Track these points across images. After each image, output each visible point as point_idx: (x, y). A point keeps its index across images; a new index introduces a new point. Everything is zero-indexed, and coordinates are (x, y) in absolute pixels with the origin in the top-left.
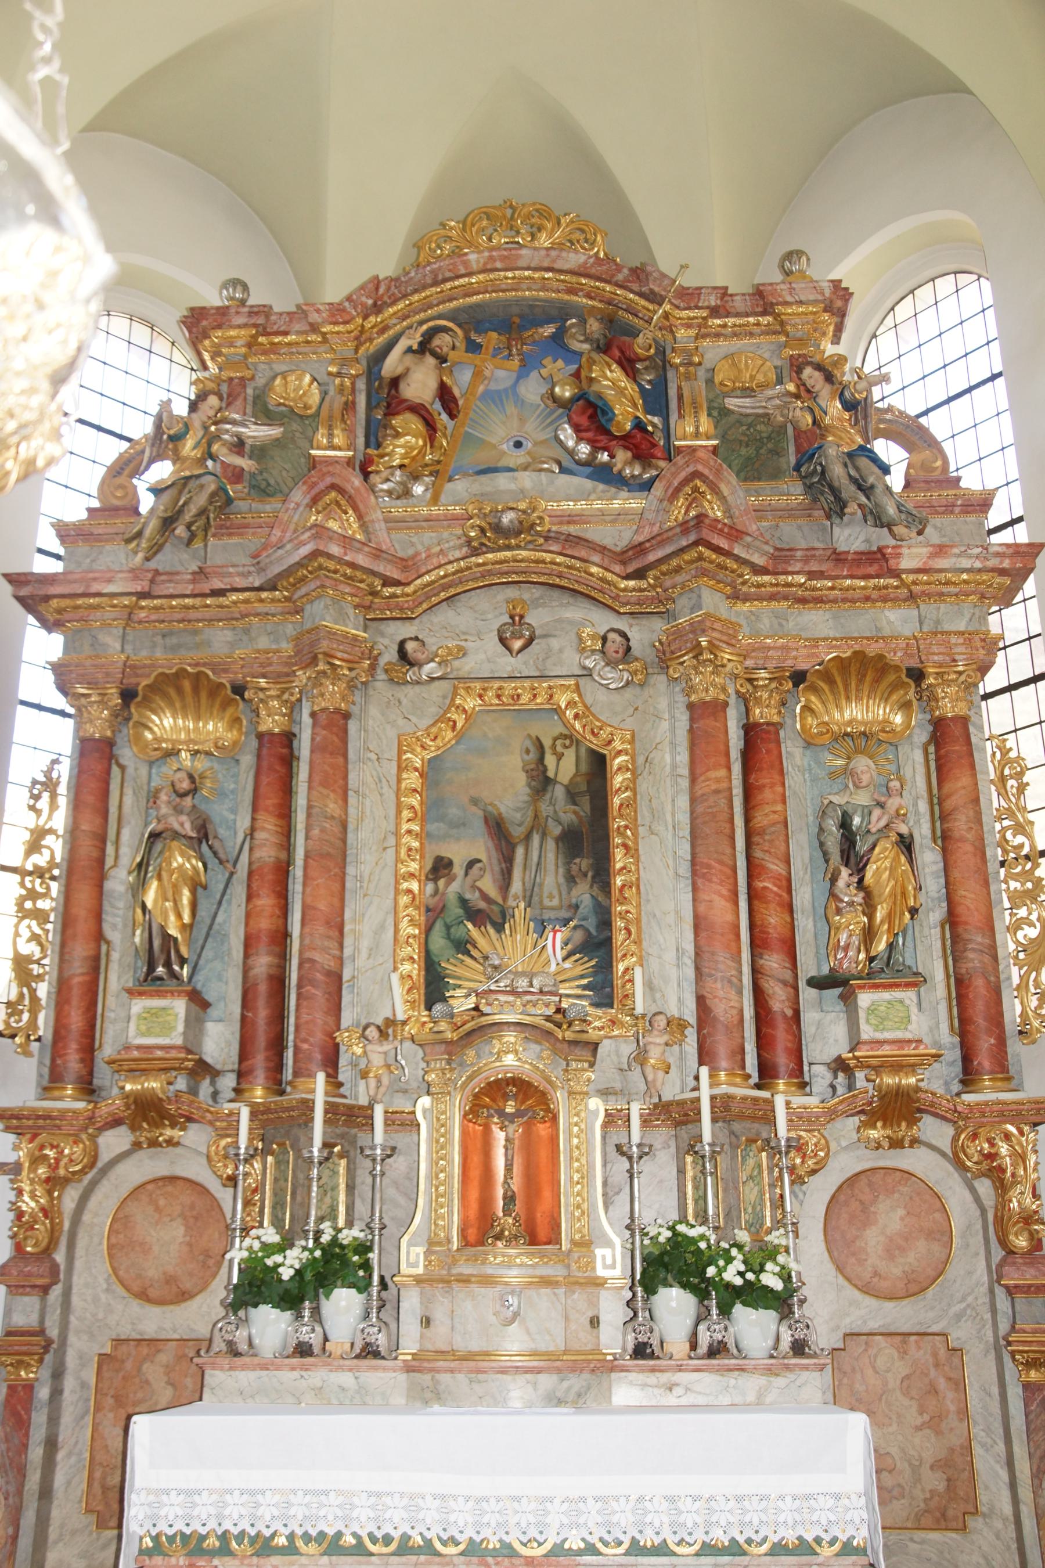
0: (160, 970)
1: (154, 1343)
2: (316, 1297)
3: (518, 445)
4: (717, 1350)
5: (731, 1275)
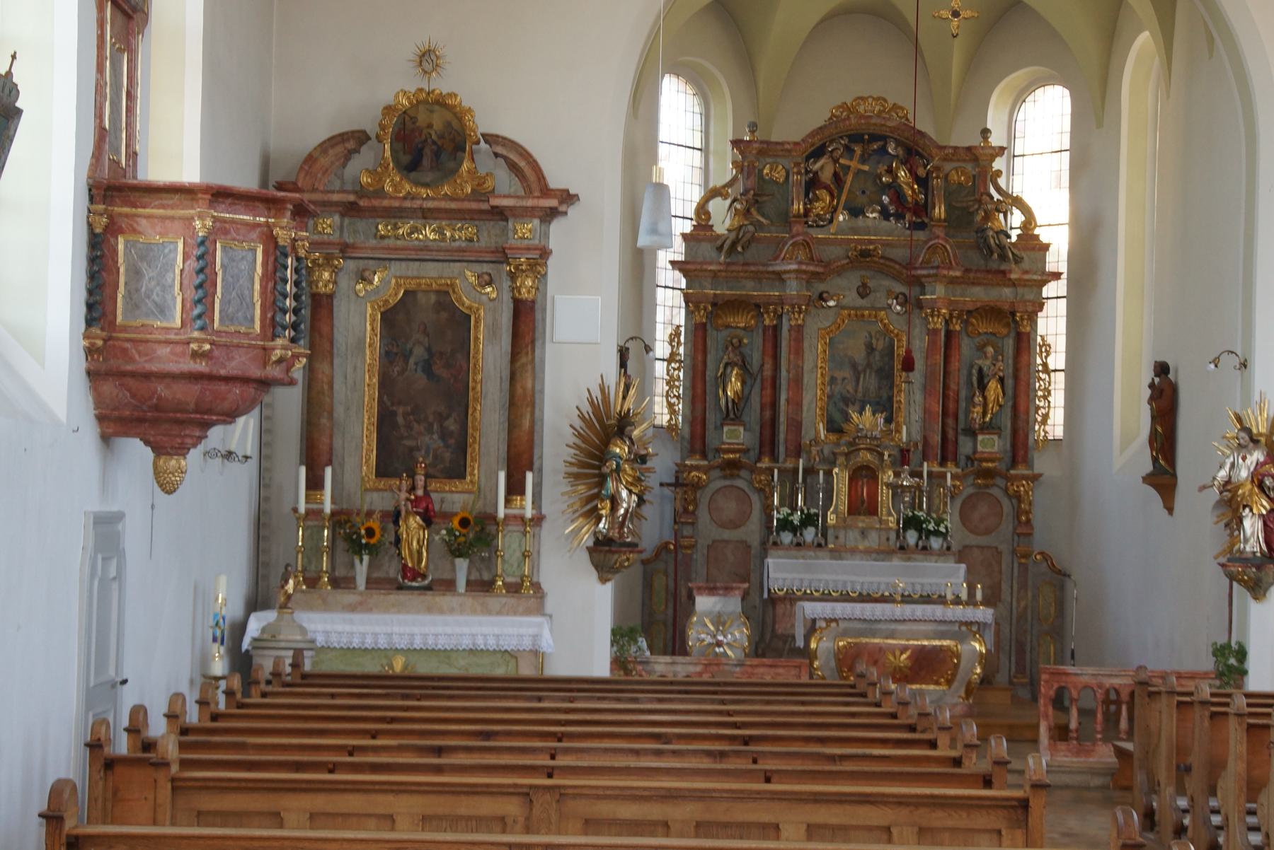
0: (732, 416)
1: (726, 542)
2: (801, 530)
3: (864, 192)
4: (924, 548)
5: (931, 527)
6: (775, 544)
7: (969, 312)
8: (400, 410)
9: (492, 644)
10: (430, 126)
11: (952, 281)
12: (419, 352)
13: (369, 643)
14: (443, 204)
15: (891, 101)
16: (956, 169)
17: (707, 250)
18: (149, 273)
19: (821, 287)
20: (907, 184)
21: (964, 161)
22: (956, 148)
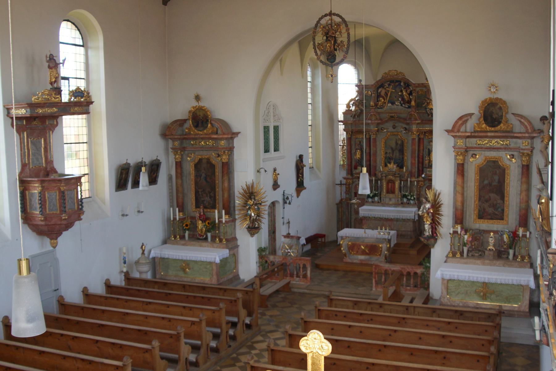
3: (396, 97)
4: (408, 203)
5: (409, 197)
6: (367, 202)
7: (425, 133)
8: (200, 190)
9: (205, 260)
10: (200, 115)
11: (418, 124)
12: (203, 175)
13: (177, 258)
14: (204, 136)
15: (399, 71)
16: (420, 90)
17: (349, 116)
18: (33, 200)
19: (382, 126)
20: (405, 95)
21: (422, 87)
22: (419, 84)
